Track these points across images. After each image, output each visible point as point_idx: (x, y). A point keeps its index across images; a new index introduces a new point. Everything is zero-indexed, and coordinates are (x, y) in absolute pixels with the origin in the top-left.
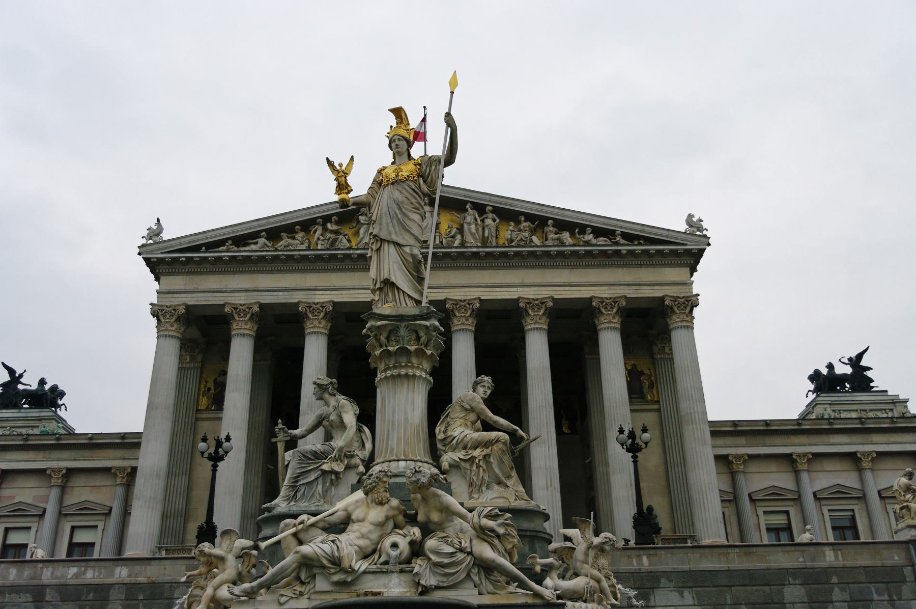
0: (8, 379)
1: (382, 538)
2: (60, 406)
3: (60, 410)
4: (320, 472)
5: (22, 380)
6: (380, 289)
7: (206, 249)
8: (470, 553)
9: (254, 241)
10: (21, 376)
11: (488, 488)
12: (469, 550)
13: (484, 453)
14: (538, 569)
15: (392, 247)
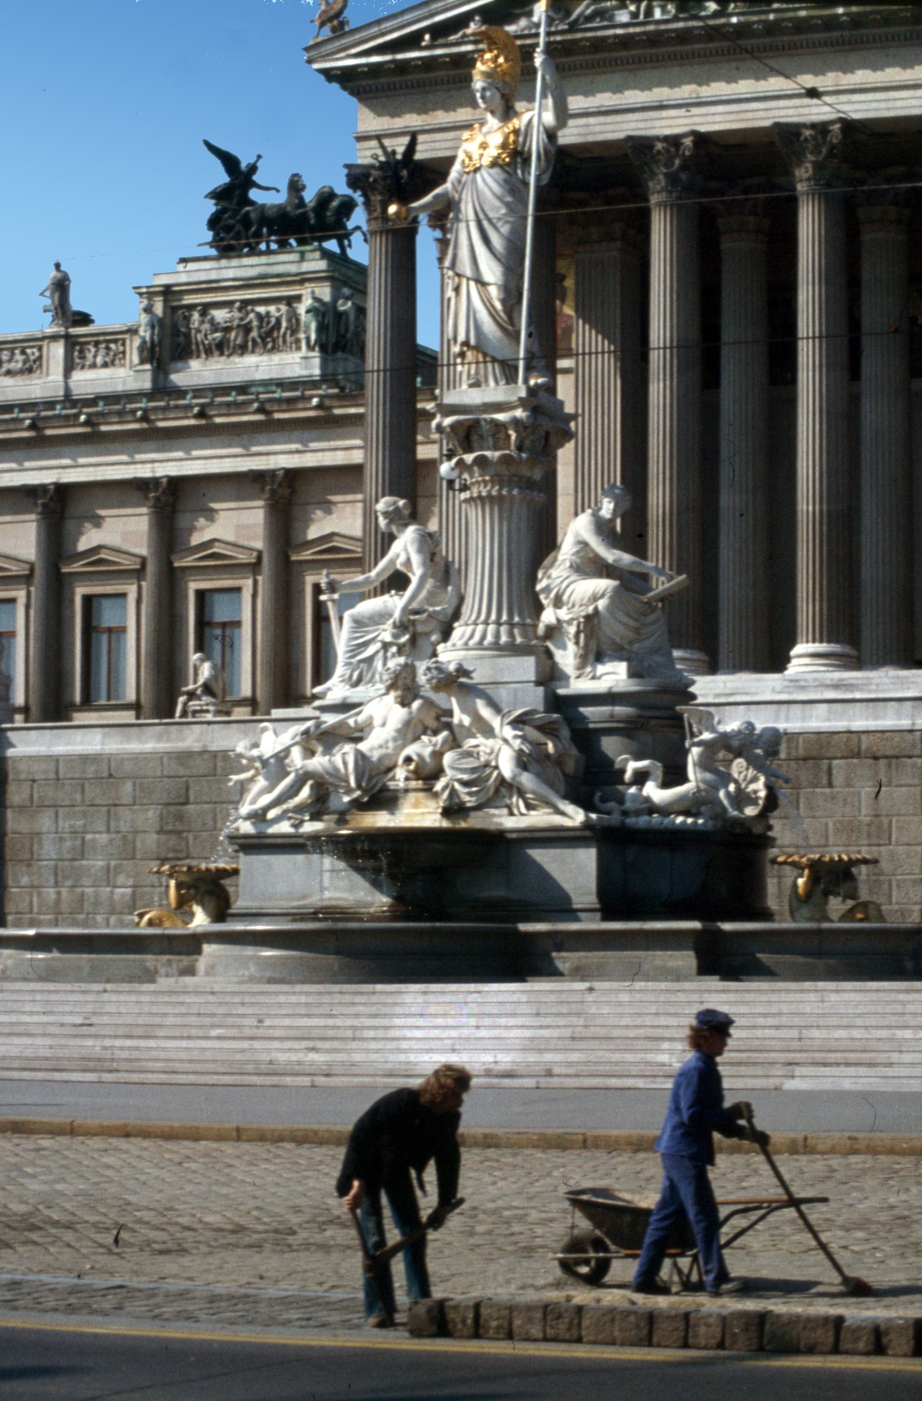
0: (222, 178)
1: (404, 746)
2: (347, 235)
3: (350, 246)
4: (378, 645)
5: (255, 178)
6: (462, 355)
7: (433, 38)
8: (496, 767)
9: (527, 9)
10: (253, 169)
11: (599, 658)
12: (493, 764)
13: (583, 613)
14: (628, 775)
15: (472, 284)
